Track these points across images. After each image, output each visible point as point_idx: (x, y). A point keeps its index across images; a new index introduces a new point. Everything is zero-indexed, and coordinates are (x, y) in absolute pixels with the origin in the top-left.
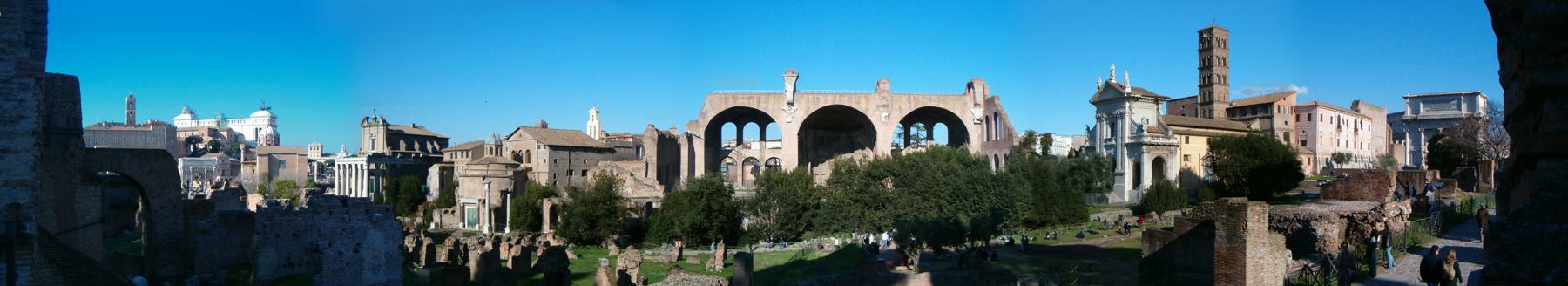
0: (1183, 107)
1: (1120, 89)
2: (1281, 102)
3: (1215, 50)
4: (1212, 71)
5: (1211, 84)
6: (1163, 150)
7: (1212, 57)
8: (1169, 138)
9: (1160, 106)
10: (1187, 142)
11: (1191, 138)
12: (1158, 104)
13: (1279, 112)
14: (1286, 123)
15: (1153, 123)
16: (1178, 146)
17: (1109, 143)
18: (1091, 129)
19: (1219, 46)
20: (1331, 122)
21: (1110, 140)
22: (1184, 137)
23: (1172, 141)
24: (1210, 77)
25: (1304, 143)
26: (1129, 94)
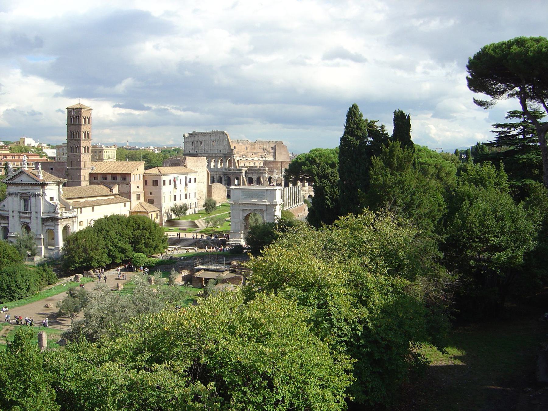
3: (82, 127)
4: (80, 144)
10: (81, 212)
14: (138, 187)
20: (170, 184)
25: (151, 202)
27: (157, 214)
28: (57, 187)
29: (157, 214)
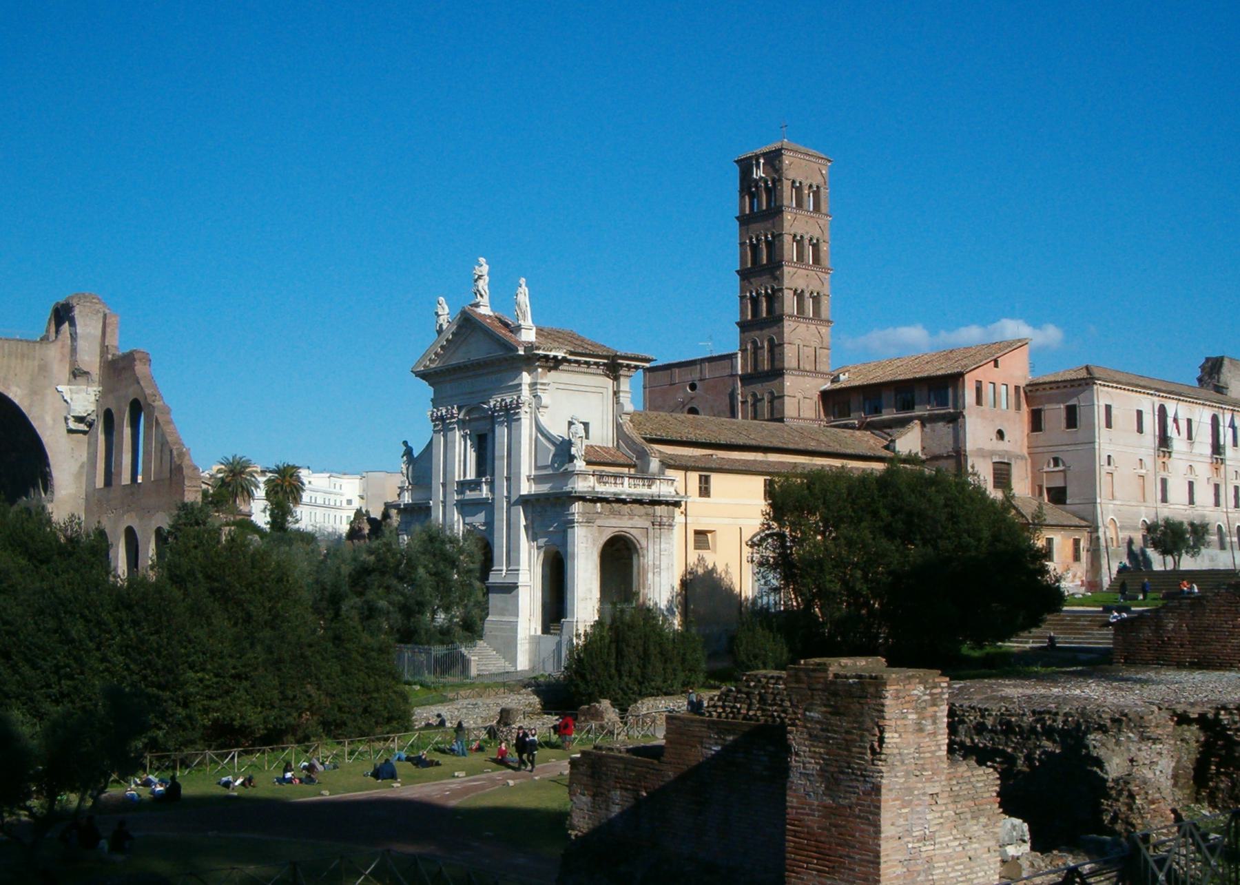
0: (693, 387)
1: (503, 332)
2: (986, 374)
3: (788, 217)
4: (779, 279)
5: (776, 319)
6: (631, 515)
7: (778, 236)
8: (651, 480)
9: (625, 385)
10: (705, 491)
11: (716, 479)
12: (616, 378)
13: (979, 401)
14: (1000, 434)
15: (602, 435)
16: (677, 504)
17: (469, 495)
18: (416, 454)
19: (800, 204)
21: (475, 485)
22: (694, 477)
23: (661, 489)
24: (774, 298)
26: (530, 347)
27: (1076, 542)
29: (1076, 542)
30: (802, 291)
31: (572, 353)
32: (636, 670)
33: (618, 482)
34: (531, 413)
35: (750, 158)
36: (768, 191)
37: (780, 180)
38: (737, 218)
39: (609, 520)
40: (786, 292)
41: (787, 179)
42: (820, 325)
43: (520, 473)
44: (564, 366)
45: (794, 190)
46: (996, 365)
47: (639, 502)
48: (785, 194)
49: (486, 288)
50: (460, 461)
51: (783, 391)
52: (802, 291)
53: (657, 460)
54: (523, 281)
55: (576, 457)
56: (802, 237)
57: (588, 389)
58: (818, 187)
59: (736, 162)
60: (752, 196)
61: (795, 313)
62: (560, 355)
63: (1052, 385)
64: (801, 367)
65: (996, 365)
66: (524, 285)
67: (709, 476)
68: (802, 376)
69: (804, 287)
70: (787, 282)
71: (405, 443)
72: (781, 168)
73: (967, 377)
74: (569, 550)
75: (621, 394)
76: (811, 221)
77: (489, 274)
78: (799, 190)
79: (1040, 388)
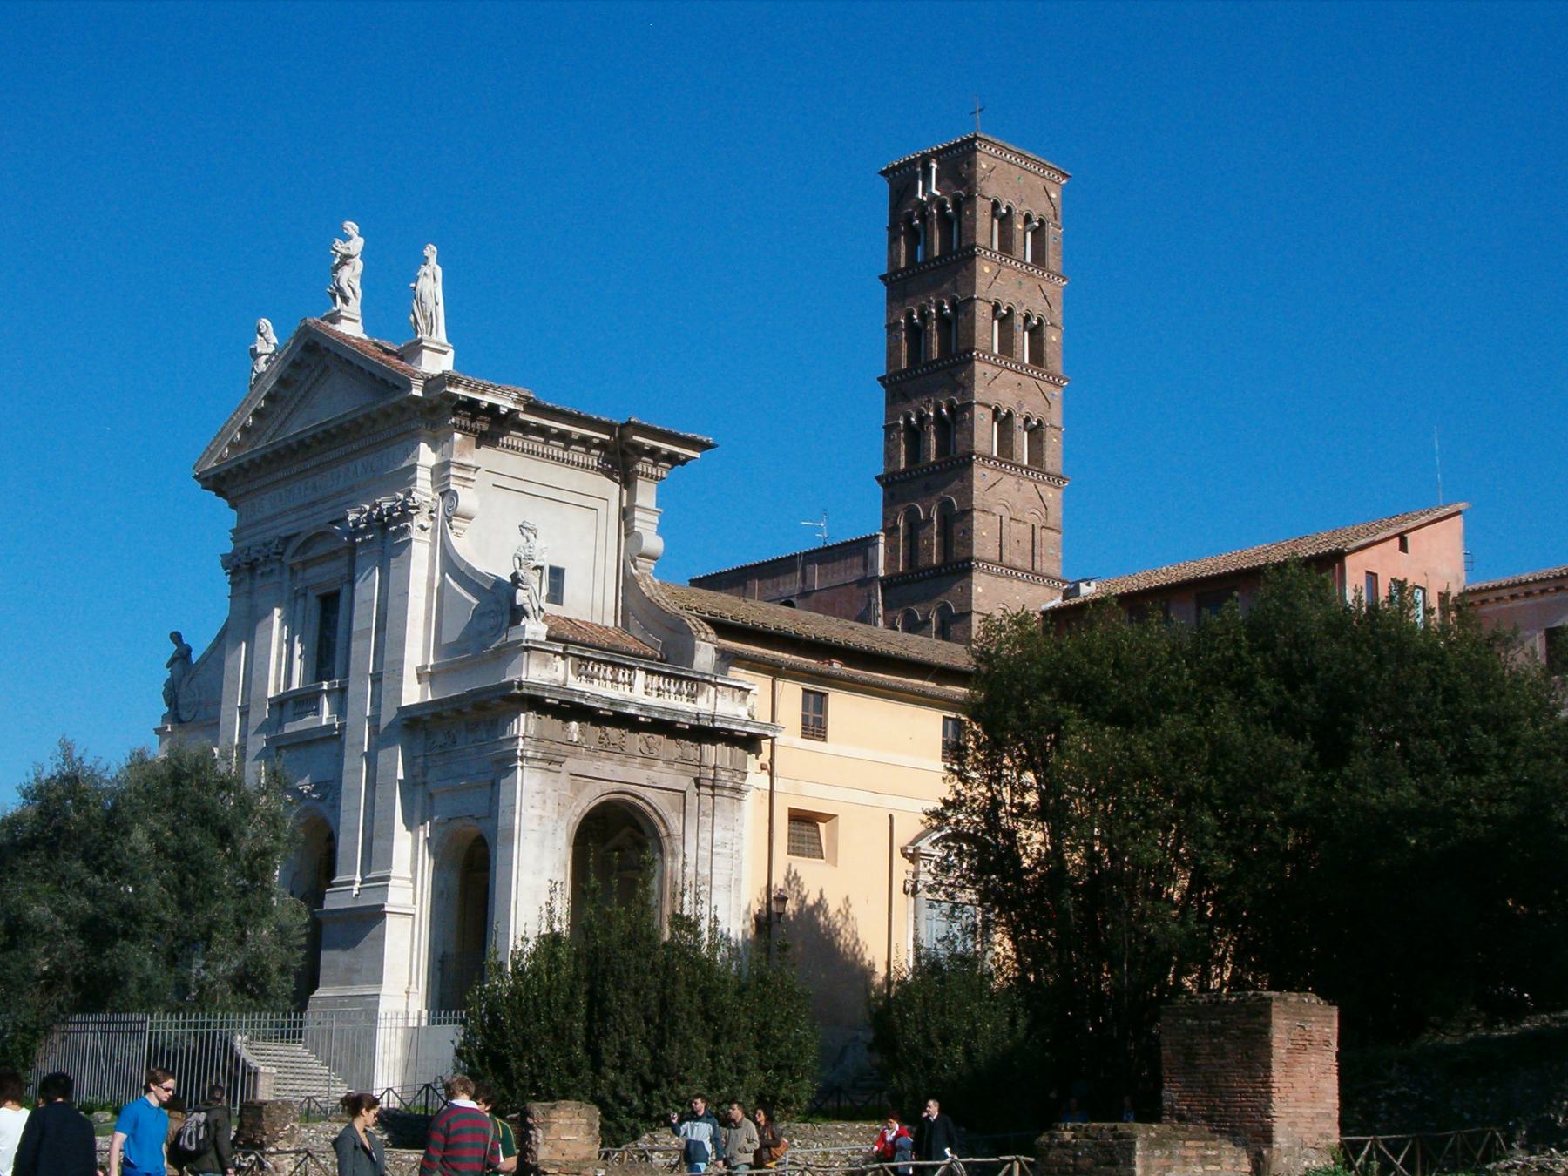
4: (966, 387)
5: (958, 463)
6: (648, 758)
7: (964, 306)
8: (696, 683)
9: (646, 494)
10: (815, 727)
16: (750, 743)
19: (1006, 246)
23: (715, 705)
24: (955, 423)
26: (435, 382)
28: (612, 489)
30: (1010, 414)
31: (533, 407)
32: (639, 1051)
33: (620, 678)
34: (434, 531)
35: (912, 162)
36: (945, 221)
37: (970, 198)
38: (883, 278)
39: (598, 764)
40: (978, 410)
41: (984, 197)
42: (1043, 482)
43: (402, 661)
44: (514, 438)
45: (996, 222)
46: (1403, 547)
47: (664, 727)
48: (978, 225)
49: (356, 284)
50: (280, 656)
51: (969, 604)
52: (1010, 414)
53: (711, 647)
54: (431, 251)
55: (526, 614)
56: (1010, 310)
57: (565, 496)
58: (1042, 222)
59: (883, 173)
60: (914, 237)
61: (995, 454)
62: (505, 404)
63: (1515, 591)
64: (1006, 559)
65: (1403, 547)
66: (433, 260)
67: (825, 695)
68: (1007, 576)
69: (1014, 407)
70: (980, 393)
71: (176, 637)
72: (972, 176)
73: (1350, 561)
74: (502, 822)
75: (637, 514)
76: (1028, 283)
77: (365, 255)
78: (1006, 221)
79: (1491, 596)
